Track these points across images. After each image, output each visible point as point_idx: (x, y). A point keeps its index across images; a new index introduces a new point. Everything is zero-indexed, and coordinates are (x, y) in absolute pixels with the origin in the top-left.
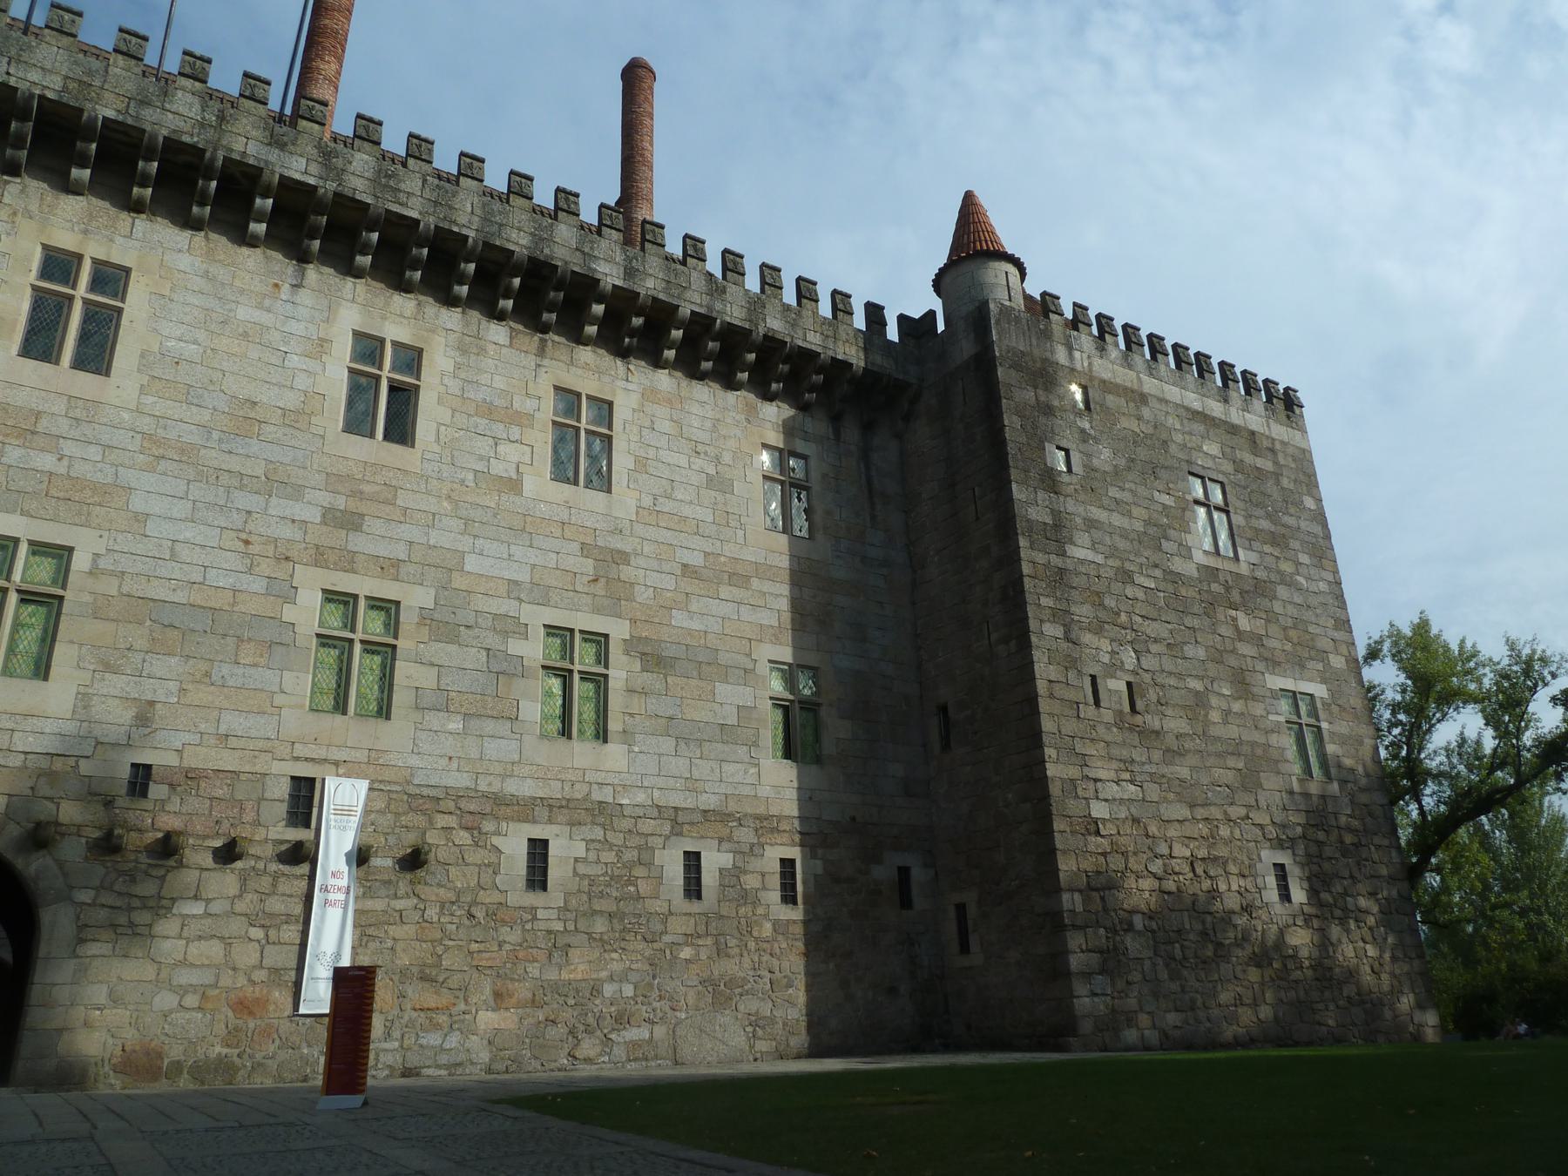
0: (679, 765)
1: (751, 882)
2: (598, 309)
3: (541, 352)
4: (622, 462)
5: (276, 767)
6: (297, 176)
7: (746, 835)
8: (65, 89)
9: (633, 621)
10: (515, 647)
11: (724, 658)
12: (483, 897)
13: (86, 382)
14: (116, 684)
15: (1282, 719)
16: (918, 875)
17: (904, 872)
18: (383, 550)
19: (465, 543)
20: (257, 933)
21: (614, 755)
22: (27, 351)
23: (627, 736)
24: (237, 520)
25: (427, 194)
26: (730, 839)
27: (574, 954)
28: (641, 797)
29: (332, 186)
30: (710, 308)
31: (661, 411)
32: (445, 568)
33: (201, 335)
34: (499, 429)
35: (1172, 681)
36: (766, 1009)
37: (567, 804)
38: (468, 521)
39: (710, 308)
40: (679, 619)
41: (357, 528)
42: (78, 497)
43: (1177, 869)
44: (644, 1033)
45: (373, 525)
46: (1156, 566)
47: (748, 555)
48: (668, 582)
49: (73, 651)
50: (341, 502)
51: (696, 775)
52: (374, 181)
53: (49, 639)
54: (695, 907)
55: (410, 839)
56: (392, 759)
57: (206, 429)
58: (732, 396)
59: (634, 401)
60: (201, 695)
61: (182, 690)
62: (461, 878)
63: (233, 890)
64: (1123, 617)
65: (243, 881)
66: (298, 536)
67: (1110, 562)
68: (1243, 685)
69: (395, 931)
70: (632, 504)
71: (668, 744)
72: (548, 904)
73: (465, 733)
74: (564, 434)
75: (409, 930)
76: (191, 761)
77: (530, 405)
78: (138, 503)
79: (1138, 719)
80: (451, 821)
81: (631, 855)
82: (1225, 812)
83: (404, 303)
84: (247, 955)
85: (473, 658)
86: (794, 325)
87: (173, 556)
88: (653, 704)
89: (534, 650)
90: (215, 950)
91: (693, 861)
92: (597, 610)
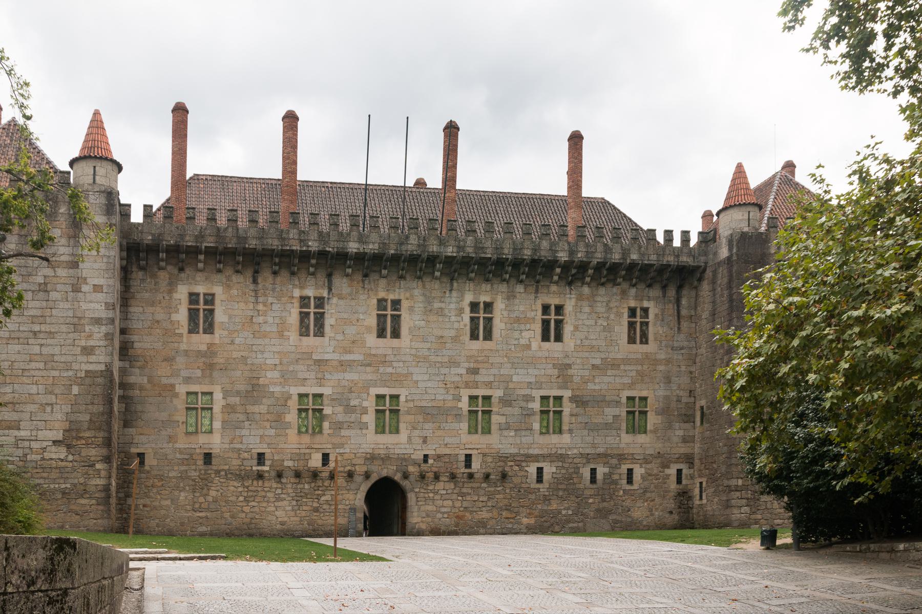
0: (589, 439)
1: (616, 477)
2: (558, 270)
3: (537, 292)
4: (568, 329)
5: (461, 452)
9: (573, 390)
10: (531, 405)
11: (607, 398)
13: (395, 342)
14: (417, 433)
17: (679, 471)
18: (486, 379)
19: (512, 372)
20: (460, 498)
21: (566, 438)
23: (570, 431)
26: (608, 463)
28: (575, 451)
31: (585, 303)
32: (506, 381)
33: (425, 317)
34: (522, 327)
36: (619, 518)
37: (550, 455)
40: (591, 386)
41: (478, 373)
42: (398, 379)
44: (575, 525)
47: (619, 356)
48: (587, 373)
50: (472, 365)
53: (398, 422)
54: (595, 486)
55: (500, 469)
56: (494, 446)
58: (615, 290)
59: (573, 301)
60: (439, 433)
62: (516, 480)
69: (497, 496)
70: (572, 345)
71: (586, 432)
72: (543, 487)
74: (546, 324)
75: (501, 496)
76: (438, 452)
77: (533, 314)
78: (415, 378)
80: (512, 463)
81: (571, 470)
83: (486, 287)
84: (458, 504)
85: (517, 411)
88: (580, 419)
89: (536, 406)
90: (450, 503)
91: (593, 471)
92: (560, 388)
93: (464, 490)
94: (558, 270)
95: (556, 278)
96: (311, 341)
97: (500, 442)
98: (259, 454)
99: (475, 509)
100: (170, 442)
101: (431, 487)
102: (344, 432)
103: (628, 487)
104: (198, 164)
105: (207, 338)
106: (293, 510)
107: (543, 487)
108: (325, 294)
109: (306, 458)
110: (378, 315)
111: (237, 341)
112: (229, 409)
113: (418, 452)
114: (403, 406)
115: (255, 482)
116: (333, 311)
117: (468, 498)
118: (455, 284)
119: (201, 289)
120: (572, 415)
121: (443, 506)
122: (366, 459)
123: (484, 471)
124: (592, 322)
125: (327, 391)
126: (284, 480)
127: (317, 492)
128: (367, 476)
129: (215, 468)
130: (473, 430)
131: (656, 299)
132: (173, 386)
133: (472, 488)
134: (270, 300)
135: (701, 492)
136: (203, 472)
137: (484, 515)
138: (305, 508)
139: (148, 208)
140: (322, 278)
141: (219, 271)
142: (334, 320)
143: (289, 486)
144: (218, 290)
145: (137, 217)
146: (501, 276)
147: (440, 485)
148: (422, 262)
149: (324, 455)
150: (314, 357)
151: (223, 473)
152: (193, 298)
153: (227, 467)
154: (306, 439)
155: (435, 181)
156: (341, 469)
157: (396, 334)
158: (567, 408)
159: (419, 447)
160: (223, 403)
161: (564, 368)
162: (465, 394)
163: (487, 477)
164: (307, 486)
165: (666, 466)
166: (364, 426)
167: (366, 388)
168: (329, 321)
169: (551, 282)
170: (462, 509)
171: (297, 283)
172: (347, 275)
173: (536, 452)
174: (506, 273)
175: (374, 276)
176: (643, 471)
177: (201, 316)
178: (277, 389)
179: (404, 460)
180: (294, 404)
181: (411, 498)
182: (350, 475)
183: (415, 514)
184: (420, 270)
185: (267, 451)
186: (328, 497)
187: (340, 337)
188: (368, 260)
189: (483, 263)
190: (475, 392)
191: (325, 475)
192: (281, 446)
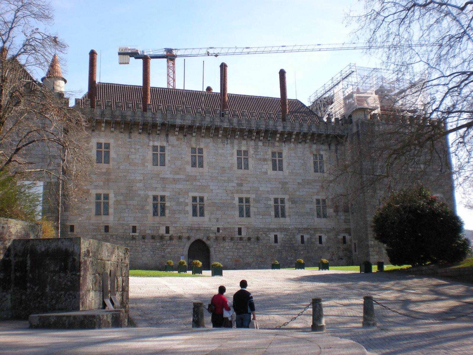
1: (313, 240)
2: (278, 135)
4: (285, 164)
6: (226, 126)
7: (312, 232)
8: (191, 122)
9: (289, 195)
10: (269, 203)
11: (306, 200)
12: (268, 244)
14: (213, 216)
16: (348, 237)
17: (344, 237)
21: (287, 220)
22: (192, 166)
23: (289, 216)
24: (225, 188)
25: (247, 123)
27: (283, 253)
28: (293, 227)
29: (231, 126)
30: (300, 130)
33: (215, 157)
37: (280, 229)
38: (259, 181)
39: (300, 130)
45: (245, 185)
47: (310, 178)
48: (295, 186)
49: (207, 212)
50: (239, 182)
51: (302, 222)
52: (238, 123)
54: (303, 245)
55: (256, 236)
57: (218, 173)
59: (287, 150)
61: (222, 216)
62: (264, 242)
63: (233, 245)
65: (234, 244)
66: (234, 189)
71: (297, 217)
72: (278, 245)
73: (263, 218)
78: (211, 188)
81: (292, 237)
83: (244, 142)
84: (236, 254)
86: (318, 129)
87: (217, 195)
89: (272, 203)
90: (231, 253)
91: (302, 237)
92: (283, 194)
93: (238, 247)
94: (278, 135)
95: (277, 139)
96: (159, 168)
97: (255, 221)
98: (133, 226)
99: (244, 257)
100: (87, 219)
101: (222, 245)
102: (177, 216)
103: (320, 245)
104: (101, 78)
105: (106, 165)
106: (151, 257)
107: (278, 245)
108: (165, 144)
109: (158, 229)
110: (192, 156)
111: (121, 167)
112: (117, 202)
113: (214, 226)
114: (206, 202)
115: (131, 242)
116: (169, 153)
117: (241, 251)
118: (229, 141)
119: (103, 141)
120: (290, 208)
121: (228, 255)
122: (188, 230)
123: (248, 236)
124: (296, 161)
125: (167, 194)
126: (146, 241)
127: (163, 247)
128: (189, 238)
129: (110, 234)
130: (241, 215)
131: (325, 150)
132: (89, 190)
133: (242, 245)
134: (138, 147)
135: (355, 248)
136: (104, 236)
137: (250, 260)
138: (157, 256)
139: (76, 100)
140: (163, 137)
141: (112, 132)
142: (170, 157)
143: (149, 244)
144: (112, 142)
145: (72, 103)
146: (251, 137)
147: (226, 244)
148: (212, 130)
149: (166, 227)
150: (161, 176)
151: (114, 237)
152: (99, 145)
153: (116, 233)
154: (158, 219)
155: (216, 89)
156: (176, 235)
157: (201, 165)
158: (287, 205)
159: (215, 224)
160: (114, 199)
161: (284, 184)
162: (237, 197)
163: (249, 239)
164: (158, 244)
165: (337, 234)
166: (187, 213)
167: (187, 193)
168: (167, 158)
169: (275, 141)
170: (238, 257)
171: (151, 138)
172: (176, 135)
173: (272, 226)
174: (253, 136)
175: (189, 136)
176: (326, 237)
177: (103, 154)
178: (142, 193)
179: (207, 230)
180: (150, 200)
181: (212, 250)
182: (180, 238)
183: (214, 259)
184: (212, 134)
185: (137, 225)
186: (169, 250)
187: (173, 166)
188: (186, 128)
189: (242, 131)
190: (242, 196)
191: (167, 238)
192: (145, 222)
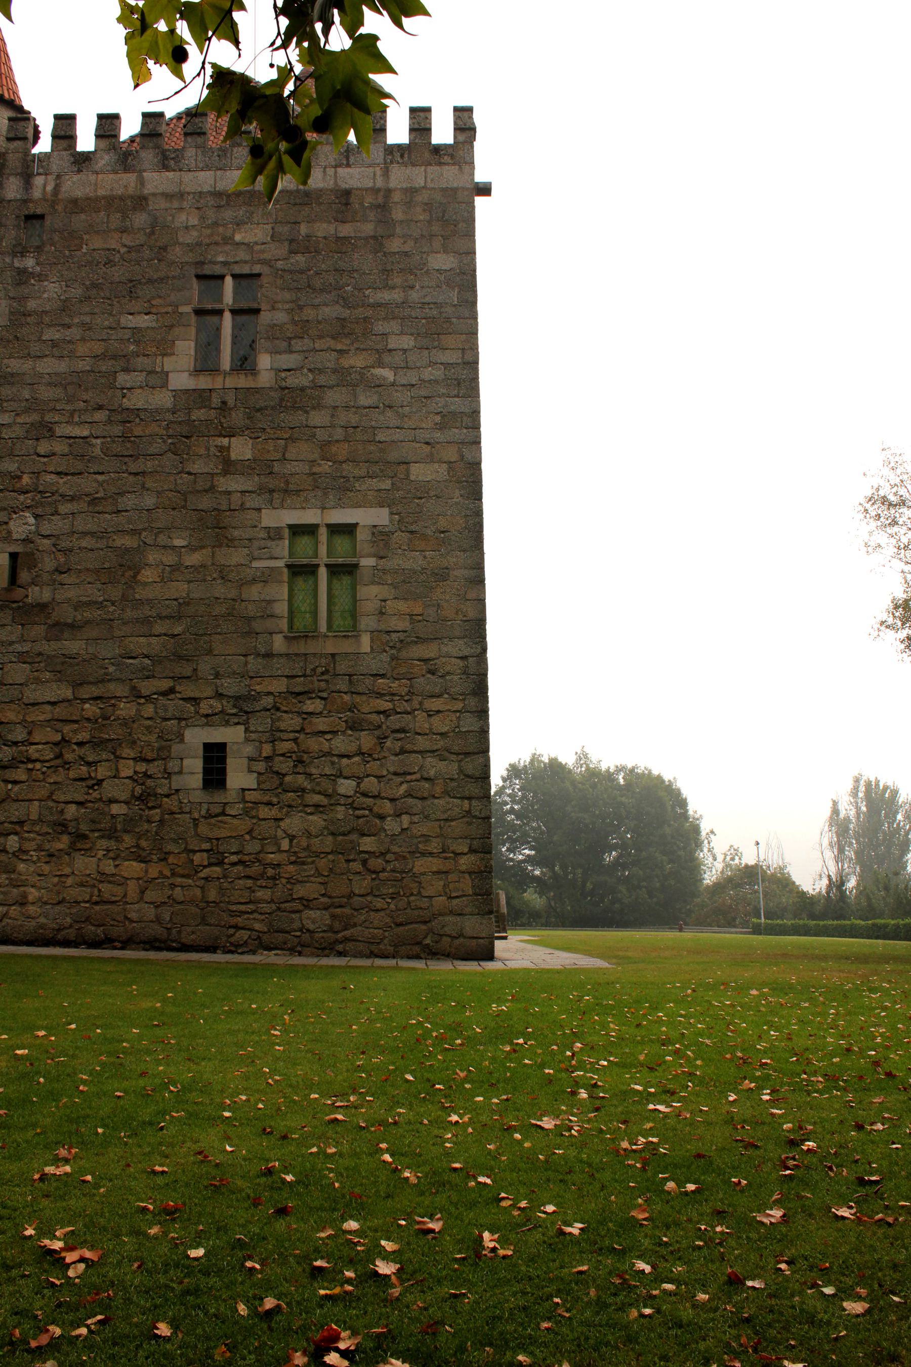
15: (280, 563)
35: (86, 543)
43: (35, 756)
46: (100, 408)
64: (26, 480)
67: (19, 420)
68: (216, 528)
79: (19, 593)
82: (134, 688)
